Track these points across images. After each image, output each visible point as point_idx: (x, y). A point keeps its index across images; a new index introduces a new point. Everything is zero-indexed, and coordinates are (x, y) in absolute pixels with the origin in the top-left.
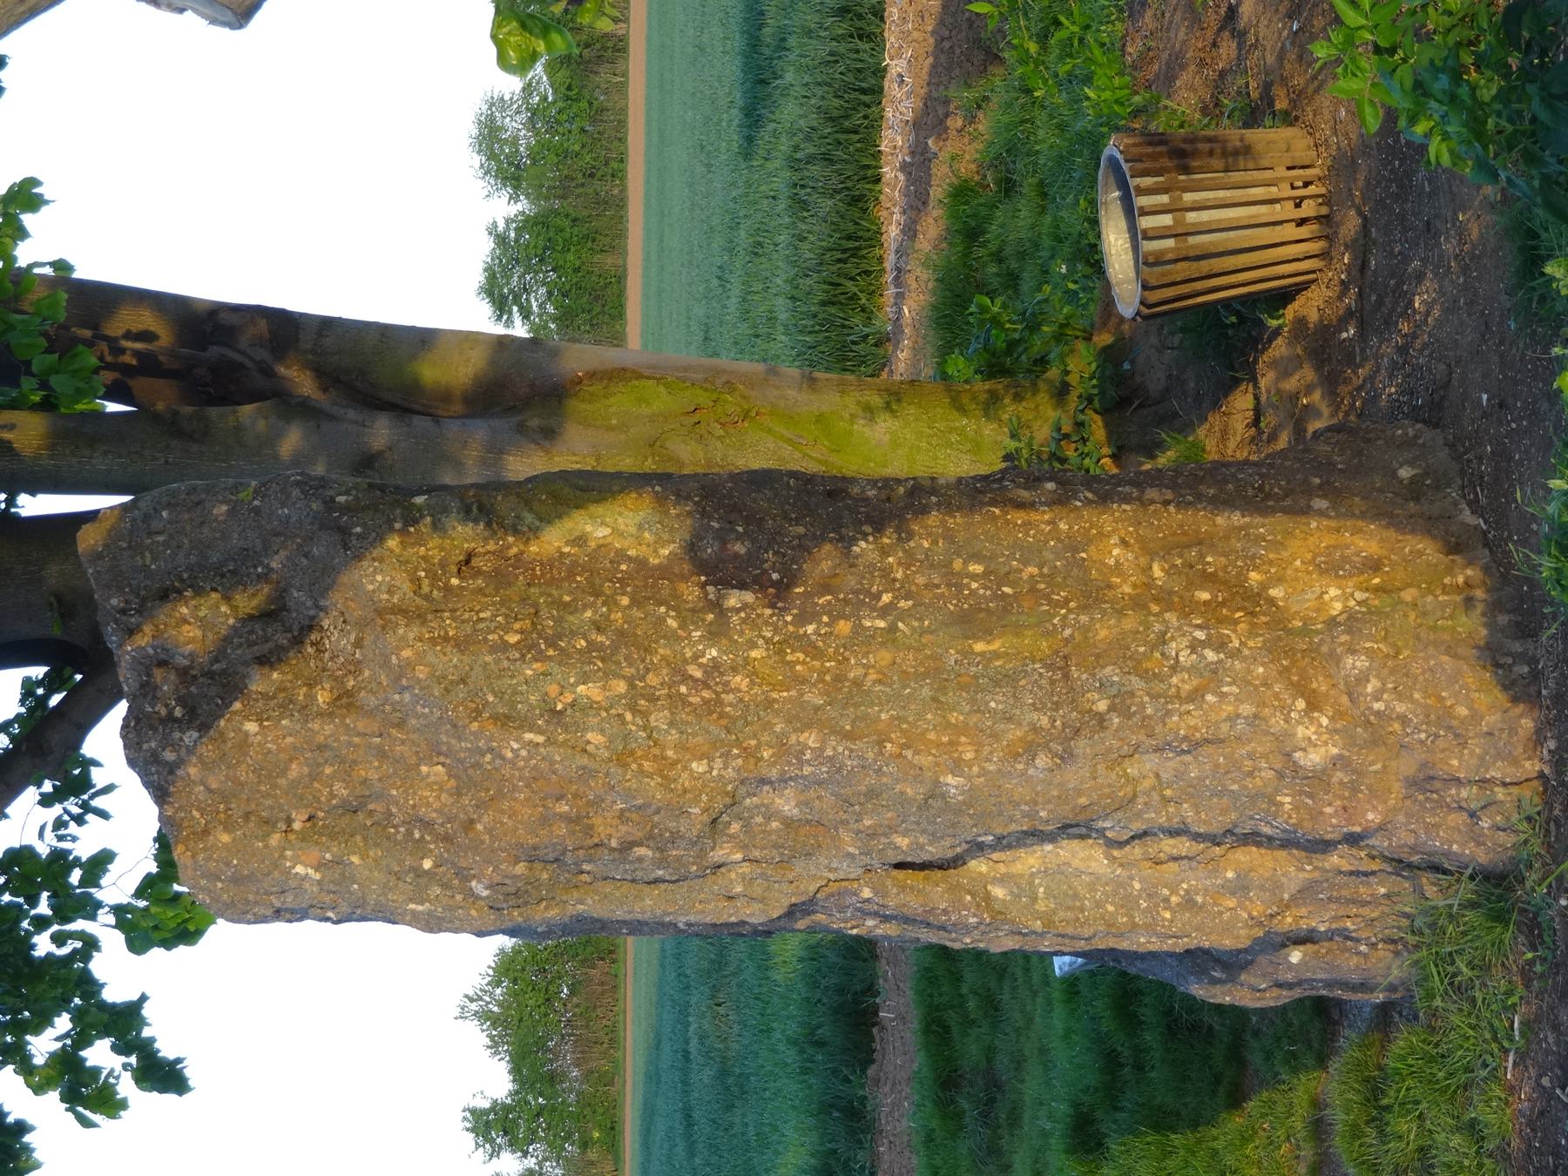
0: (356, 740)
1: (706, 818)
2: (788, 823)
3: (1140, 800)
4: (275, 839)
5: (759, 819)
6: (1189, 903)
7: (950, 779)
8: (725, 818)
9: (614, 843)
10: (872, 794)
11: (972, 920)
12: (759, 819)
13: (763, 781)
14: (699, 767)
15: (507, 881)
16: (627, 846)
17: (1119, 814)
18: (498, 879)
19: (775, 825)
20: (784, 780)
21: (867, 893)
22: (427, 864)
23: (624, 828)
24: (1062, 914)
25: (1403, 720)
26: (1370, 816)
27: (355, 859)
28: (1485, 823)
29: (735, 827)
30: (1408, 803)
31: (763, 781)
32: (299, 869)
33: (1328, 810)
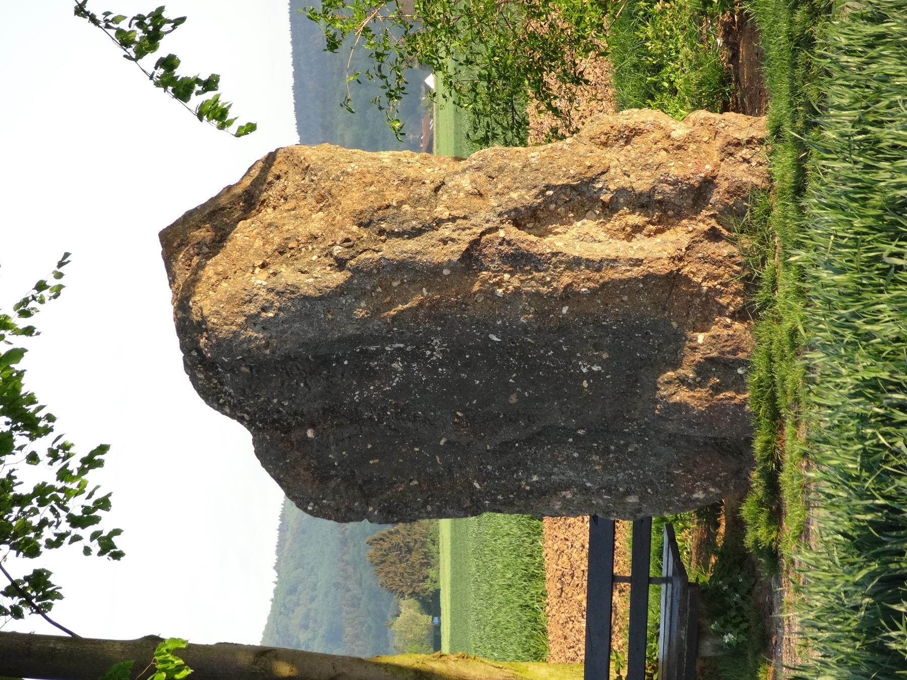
0: (285, 214)
1: (432, 186)
2: (469, 194)
3: (612, 171)
4: (248, 274)
5: (455, 192)
6: (642, 249)
7: (533, 154)
8: (440, 192)
9: (394, 204)
10: (501, 169)
11: (548, 251)
12: (455, 192)
13: (456, 173)
14: (428, 170)
15: (350, 236)
16: (401, 203)
17: (603, 177)
18: (346, 236)
19: (462, 194)
20: (464, 171)
21: (502, 234)
22: (315, 258)
23: (398, 194)
24: (587, 253)
25: (715, 119)
26: (707, 167)
27: (283, 270)
28: (754, 164)
29: (445, 197)
30: (722, 164)
31: (456, 173)
32: (259, 282)
33: (690, 165)
